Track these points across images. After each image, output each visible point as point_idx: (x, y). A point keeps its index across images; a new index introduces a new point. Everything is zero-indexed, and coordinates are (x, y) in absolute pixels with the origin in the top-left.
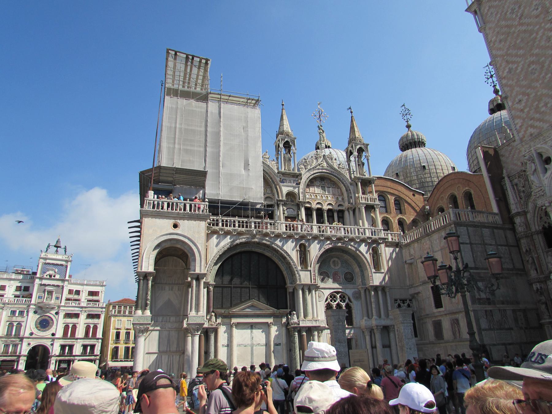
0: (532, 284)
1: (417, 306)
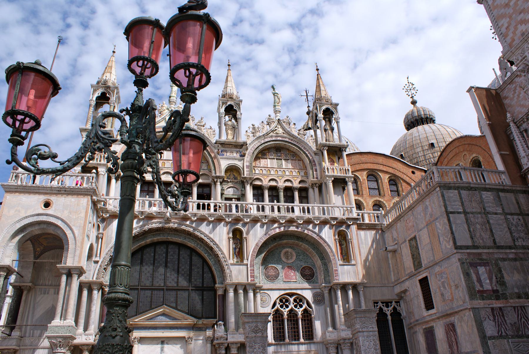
1: (406, 310)
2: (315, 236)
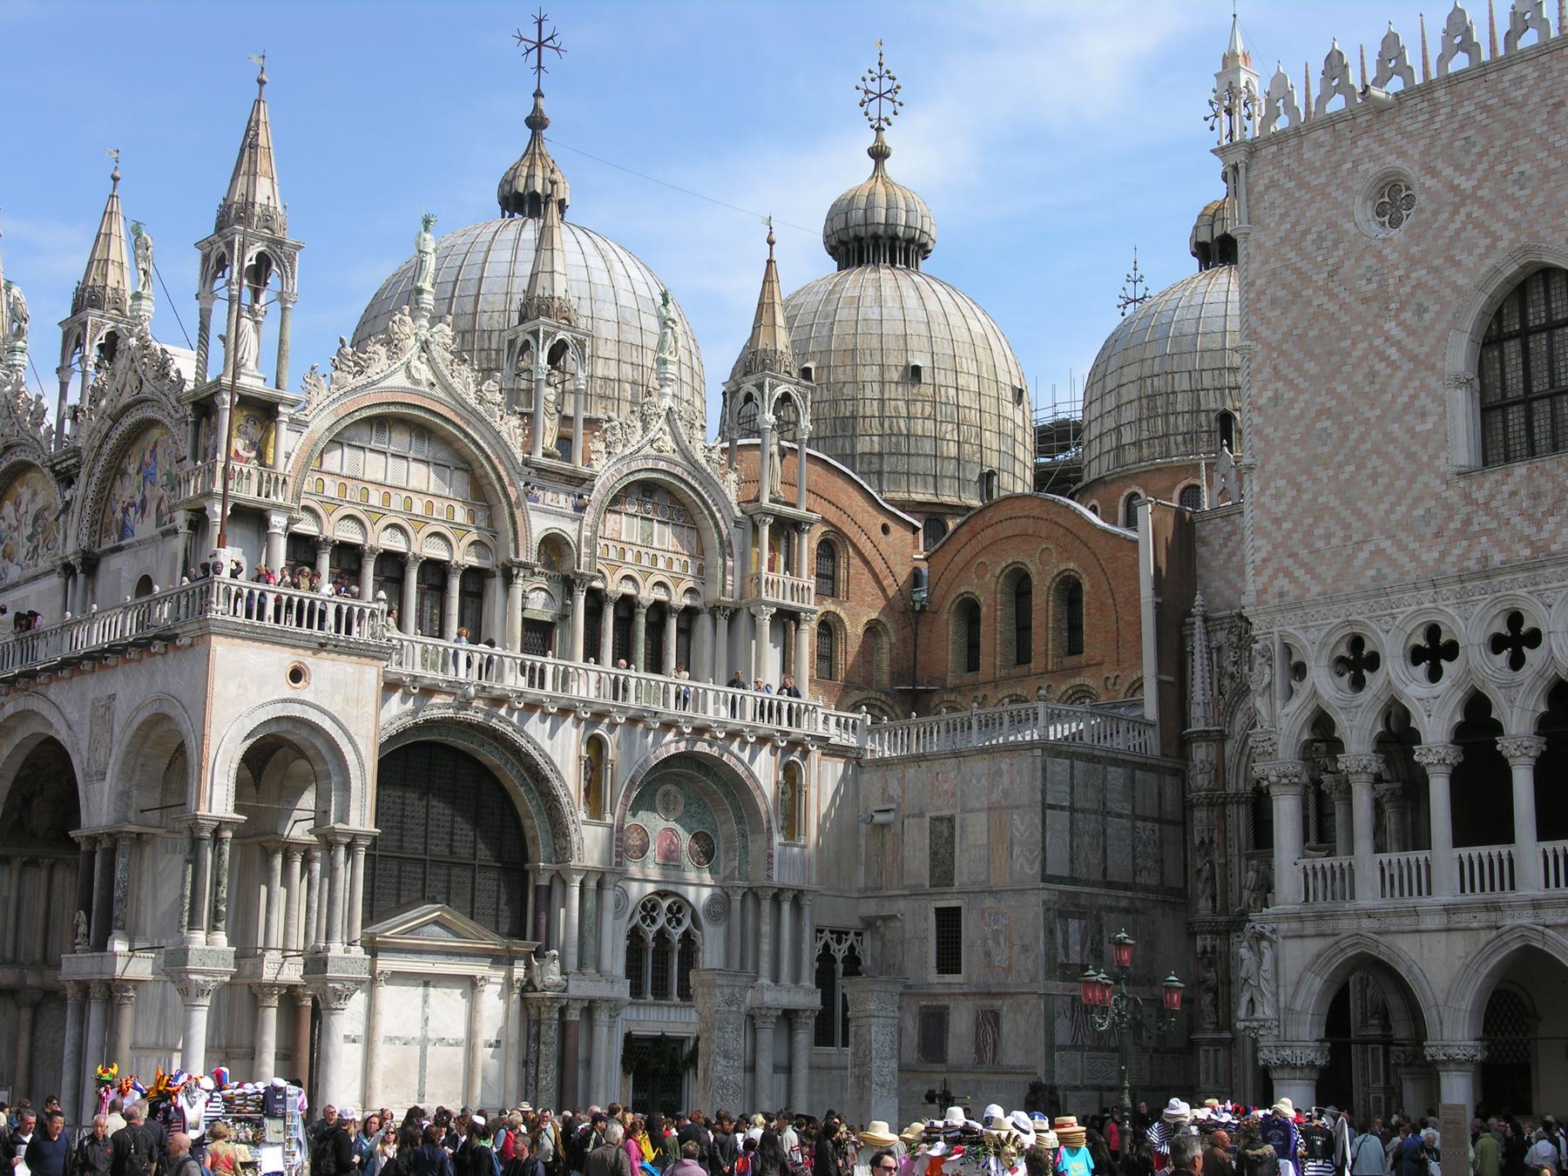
0: (1195, 934)
2: (740, 770)
